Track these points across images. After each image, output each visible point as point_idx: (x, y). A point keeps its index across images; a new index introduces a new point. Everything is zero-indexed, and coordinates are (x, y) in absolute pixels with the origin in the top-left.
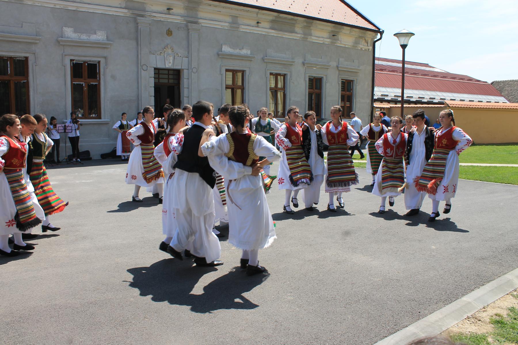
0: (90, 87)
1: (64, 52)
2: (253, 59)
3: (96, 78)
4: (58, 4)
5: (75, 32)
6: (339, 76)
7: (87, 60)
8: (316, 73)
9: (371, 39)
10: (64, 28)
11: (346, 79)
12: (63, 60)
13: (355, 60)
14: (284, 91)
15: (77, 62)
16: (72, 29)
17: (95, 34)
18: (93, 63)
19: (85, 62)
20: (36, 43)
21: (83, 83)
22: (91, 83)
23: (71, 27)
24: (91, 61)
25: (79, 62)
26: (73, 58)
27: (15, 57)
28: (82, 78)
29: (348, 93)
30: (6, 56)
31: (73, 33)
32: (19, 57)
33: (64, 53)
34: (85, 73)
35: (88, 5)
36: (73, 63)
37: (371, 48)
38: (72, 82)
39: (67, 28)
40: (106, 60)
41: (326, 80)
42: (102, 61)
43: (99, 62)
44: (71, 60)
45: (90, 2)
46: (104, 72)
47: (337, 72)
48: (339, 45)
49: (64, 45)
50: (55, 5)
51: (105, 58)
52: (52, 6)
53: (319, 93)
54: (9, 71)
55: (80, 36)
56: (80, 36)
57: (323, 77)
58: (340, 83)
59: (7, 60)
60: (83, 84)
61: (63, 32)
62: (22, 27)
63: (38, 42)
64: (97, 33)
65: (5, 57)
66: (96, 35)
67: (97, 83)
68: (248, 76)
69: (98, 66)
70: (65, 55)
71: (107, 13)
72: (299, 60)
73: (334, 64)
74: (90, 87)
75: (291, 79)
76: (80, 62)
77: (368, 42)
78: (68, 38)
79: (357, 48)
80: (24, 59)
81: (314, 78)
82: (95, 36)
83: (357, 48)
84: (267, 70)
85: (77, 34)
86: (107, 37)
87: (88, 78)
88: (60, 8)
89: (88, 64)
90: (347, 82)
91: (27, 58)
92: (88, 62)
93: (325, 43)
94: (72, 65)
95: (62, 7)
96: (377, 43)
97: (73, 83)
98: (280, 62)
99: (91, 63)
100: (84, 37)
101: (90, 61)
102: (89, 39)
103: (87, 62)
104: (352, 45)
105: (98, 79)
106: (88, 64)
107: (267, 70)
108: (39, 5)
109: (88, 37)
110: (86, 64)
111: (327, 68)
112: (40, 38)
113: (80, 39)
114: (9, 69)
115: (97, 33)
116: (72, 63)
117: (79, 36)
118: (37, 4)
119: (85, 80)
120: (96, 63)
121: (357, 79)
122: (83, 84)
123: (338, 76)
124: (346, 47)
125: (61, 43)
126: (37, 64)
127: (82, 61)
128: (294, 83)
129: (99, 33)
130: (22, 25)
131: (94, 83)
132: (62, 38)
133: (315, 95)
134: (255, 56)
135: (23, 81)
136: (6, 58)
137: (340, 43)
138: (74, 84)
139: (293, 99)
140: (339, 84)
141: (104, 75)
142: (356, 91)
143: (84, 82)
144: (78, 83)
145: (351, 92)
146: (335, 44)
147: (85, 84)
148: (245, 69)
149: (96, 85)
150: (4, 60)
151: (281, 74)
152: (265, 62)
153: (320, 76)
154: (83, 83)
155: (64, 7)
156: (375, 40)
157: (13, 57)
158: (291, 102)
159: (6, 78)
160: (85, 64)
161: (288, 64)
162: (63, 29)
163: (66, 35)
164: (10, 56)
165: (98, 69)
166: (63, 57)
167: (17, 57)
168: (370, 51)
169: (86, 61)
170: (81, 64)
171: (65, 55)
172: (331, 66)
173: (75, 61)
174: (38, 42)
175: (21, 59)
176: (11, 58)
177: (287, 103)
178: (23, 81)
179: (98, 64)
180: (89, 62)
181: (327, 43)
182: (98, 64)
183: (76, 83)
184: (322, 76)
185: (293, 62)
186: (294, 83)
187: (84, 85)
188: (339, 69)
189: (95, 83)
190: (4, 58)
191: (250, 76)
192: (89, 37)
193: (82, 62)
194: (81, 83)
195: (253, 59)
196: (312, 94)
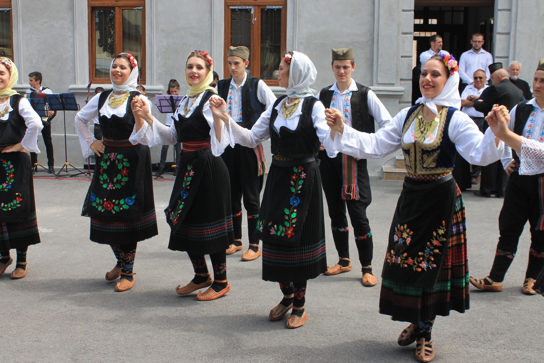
21: (251, 7)
22: (268, 7)
38: (227, 5)
60: (250, 9)
97: (231, 7)
122: (250, 9)
131: (274, 7)
138: (231, 9)
143: (254, 6)
144: (240, 8)
147: (254, 10)
149: (279, 10)
154: (251, 7)
183: (237, 7)
187: (252, 12)
189: (277, 7)
194: (248, 7)
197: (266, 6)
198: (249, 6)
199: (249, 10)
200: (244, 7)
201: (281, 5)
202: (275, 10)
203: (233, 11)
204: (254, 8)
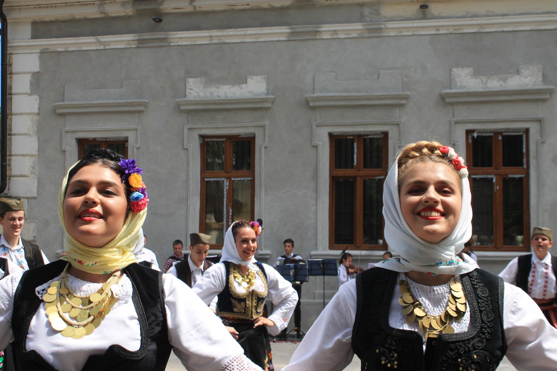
0: (506, 182)
1: (453, 117)
3: (521, 164)
4: (443, 26)
5: (477, 74)
7: (502, 129)
10: (455, 70)
12: (450, 133)
15: (481, 134)
16: (469, 70)
17: (518, 72)
18: (514, 134)
19: (497, 133)
20: (402, 106)
21: (492, 176)
22: (510, 176)
23: (469, 66)
24: (511, 131)
25: (485, 135)
26: (470, 127)
27: (366, 133)
28: (490, 165)
30: (352, 134)
31: (471, 78)
32: (372, 134)
33: (453, 119)
34: (498, 155)
35: (500, 17)
36: (473, 137)
39: (460, 69)
40: (541, 125)
42: (534, 128)
43: (527, 131)
44: (469, 132)
45: (507, 12)
46: (537, 151)
49: (453, 104)
50: (438, 30)
51: (539, 121)
52: (433, 32)
54: (355, 160)
55: (487, 81)
56: (487, 81)
59: (352, 141)
60: (492, 179)
61: (452, 77)
62: (379, 78)
63: (404, 102)
64: (522, 71)
65: (350, 136)
66: (518, 76)
67: (523, 176)
69: (524, 139)
70: (456, 123)
71: (543, 28)
74: (506, 182)
76: (488, 134)
78: (461, 87)
80: (382, 136)
82: (517, 78)
85: (481, 79)
86: (544, 77)
87: (504, 165)
88: (447, 34)
89: (504, 137)
91: (386, 134)
92: (504, 134)
94: (470, 141)
95: (451, 30)
99: (510, 134)
100: (494, 84)
101: (507, 130)
102: (504, 85)
103: (501, 133)
105: (525, 166)
106: (504, 137)
108: (410, 33)
109: (501, 83)
110: (500, 138)
112: (408, 95)
113: (486, 88)
114: (355, 156)
115: (522, 71)
116: (470, 137)
117: (484, 82)
118: (406, 34)
119: (498, 170)
120: (521, 134)
122: (492, 179)
125: (448, 100)
126: (401, 143)
127: (491, 132)
129: (527, 72)
130: (379, 74)
131: (516, 176)
132: (450, 89)
135: (377, 178)
136: (351, 137)
141: (537, 157)
143: (496, 175)
144: (482, 176)
147: (496, 179)
149: (521, 179)
150: (347, 140)
154: (492, 176)
155: (454, 30)
157: (362, 134)
159: (349, 172)
160: (498, 137)
162: (452, 73)
163: (458, 84)
164: (359, 133)
165: (524, 146)
166: (450, 127)
167: (369, 134)
169: (500, 131)
170: (490, 137)
171: (456, 123)
173: (477, 133)
174: (404, 102)
175: (376, 137)
176: (359, 136)
178: (377, 178)
179: (524, 136)
180: (505, 132)
182: (524, 136)
183: (478, 176)
187: (494, 181)
189: (519, 176)
190: (348, 137)
192: (505, 80)
193: (492, 134)
194: (490, 176)
197: (507, 175)
198: (491, 174)
199: (490, 179)
200: (486, 176)
201: (523, 174)
202: (517, 178)
203: (475, 180)
204: (496, 177)
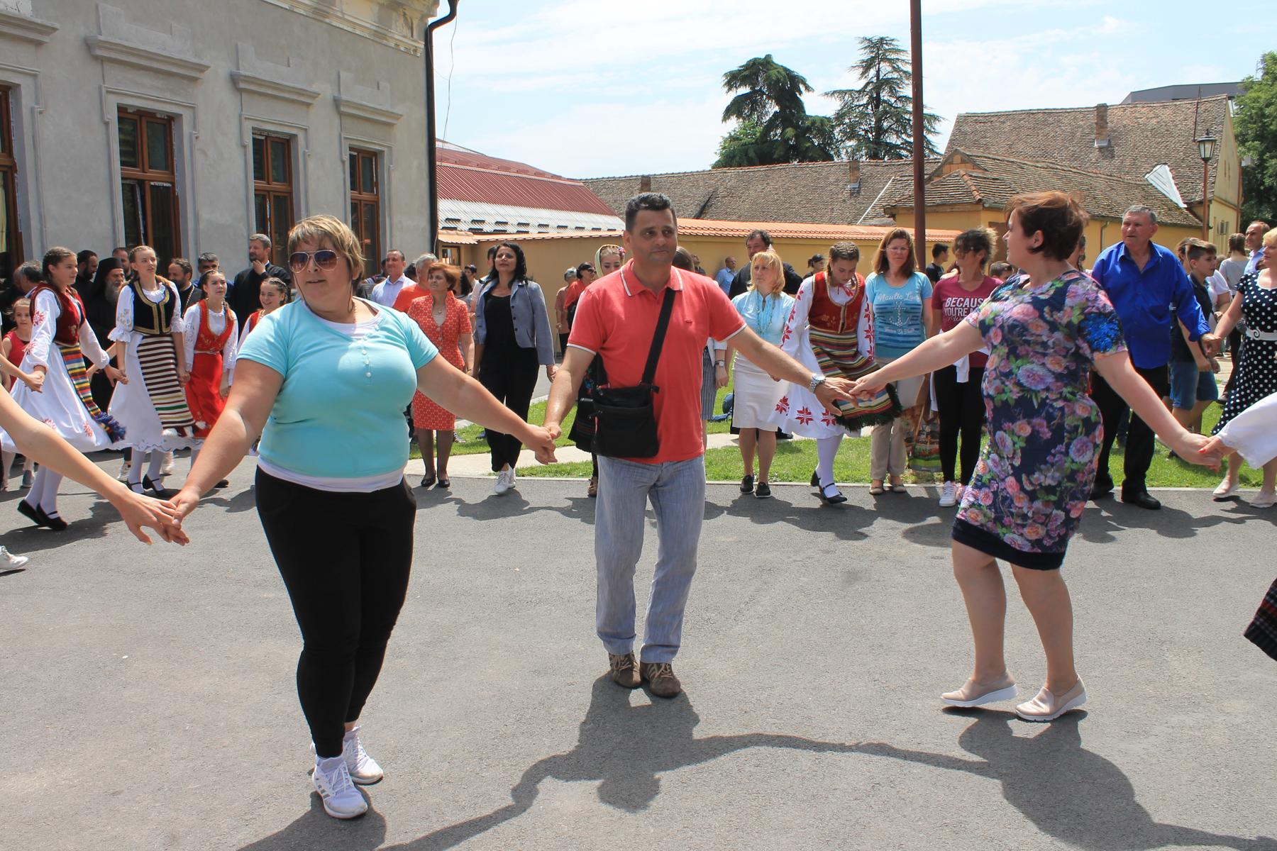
2: (46, 39)
6: (343, 136)
8: (277, 119)
9: (420, 16)
11: (362, 144)
13: (381, 83)
14: (173, 184)
29: (366, 196)
37: (421, 45)
41: (307, 148)
47: (337, 121)
48: (338, 25)
53: (286, 195)
57: (295, 136)
58: (346, 158)
68: (32, 110)
72: (219, 68)
73: (326, 91)
75: (197, 138)
77: (412, 24)
79: (385, 42)
81: (267, 137)
83: (385, 42)
84: (108, 92)
90: (363, 157)
93: (295, 10)
96: (436, 33)
98: (155, 65)
104: (375, 28)
107: (108, 92)
111: (308, 105)
121: (390, 148)
123: (340, 135)
124: (358, 32)
128: (204, 153)
133: (272, 200)
134: (57, 25)
137: (340, 15)
139: (205, 215)
140: (343, 162)
142: (389, 190)
145: (373, 191)
146: (327, 20)
148: (16, 81)
151: (159, 116)
152: (96, 58)
153: (287, 130)
156: (431, 20)
158: (202, 226)
161: (189, 74)
168: (419, 55)
172: (319, 94)
177: (186, 231)
181: (302, 12)
184: (293, 131)
185: (202, 68)
186: (204, 153)
188: (343, 109)
191: (41, 113)
195: (46, 39)
196: (264, 196)
